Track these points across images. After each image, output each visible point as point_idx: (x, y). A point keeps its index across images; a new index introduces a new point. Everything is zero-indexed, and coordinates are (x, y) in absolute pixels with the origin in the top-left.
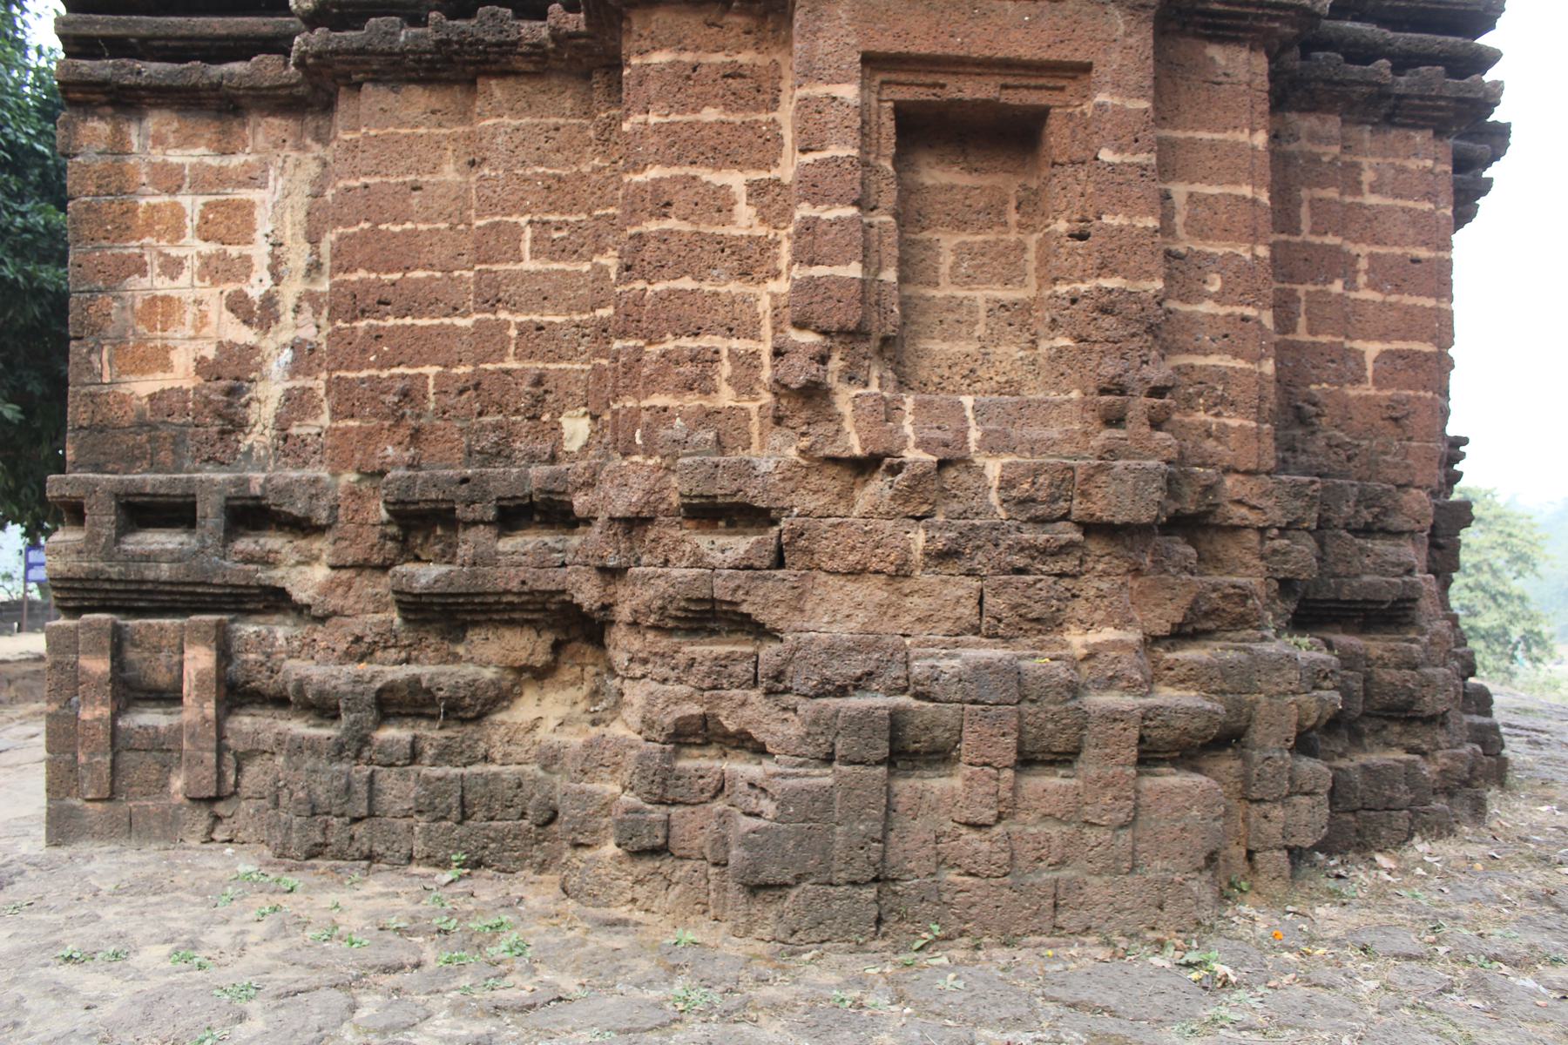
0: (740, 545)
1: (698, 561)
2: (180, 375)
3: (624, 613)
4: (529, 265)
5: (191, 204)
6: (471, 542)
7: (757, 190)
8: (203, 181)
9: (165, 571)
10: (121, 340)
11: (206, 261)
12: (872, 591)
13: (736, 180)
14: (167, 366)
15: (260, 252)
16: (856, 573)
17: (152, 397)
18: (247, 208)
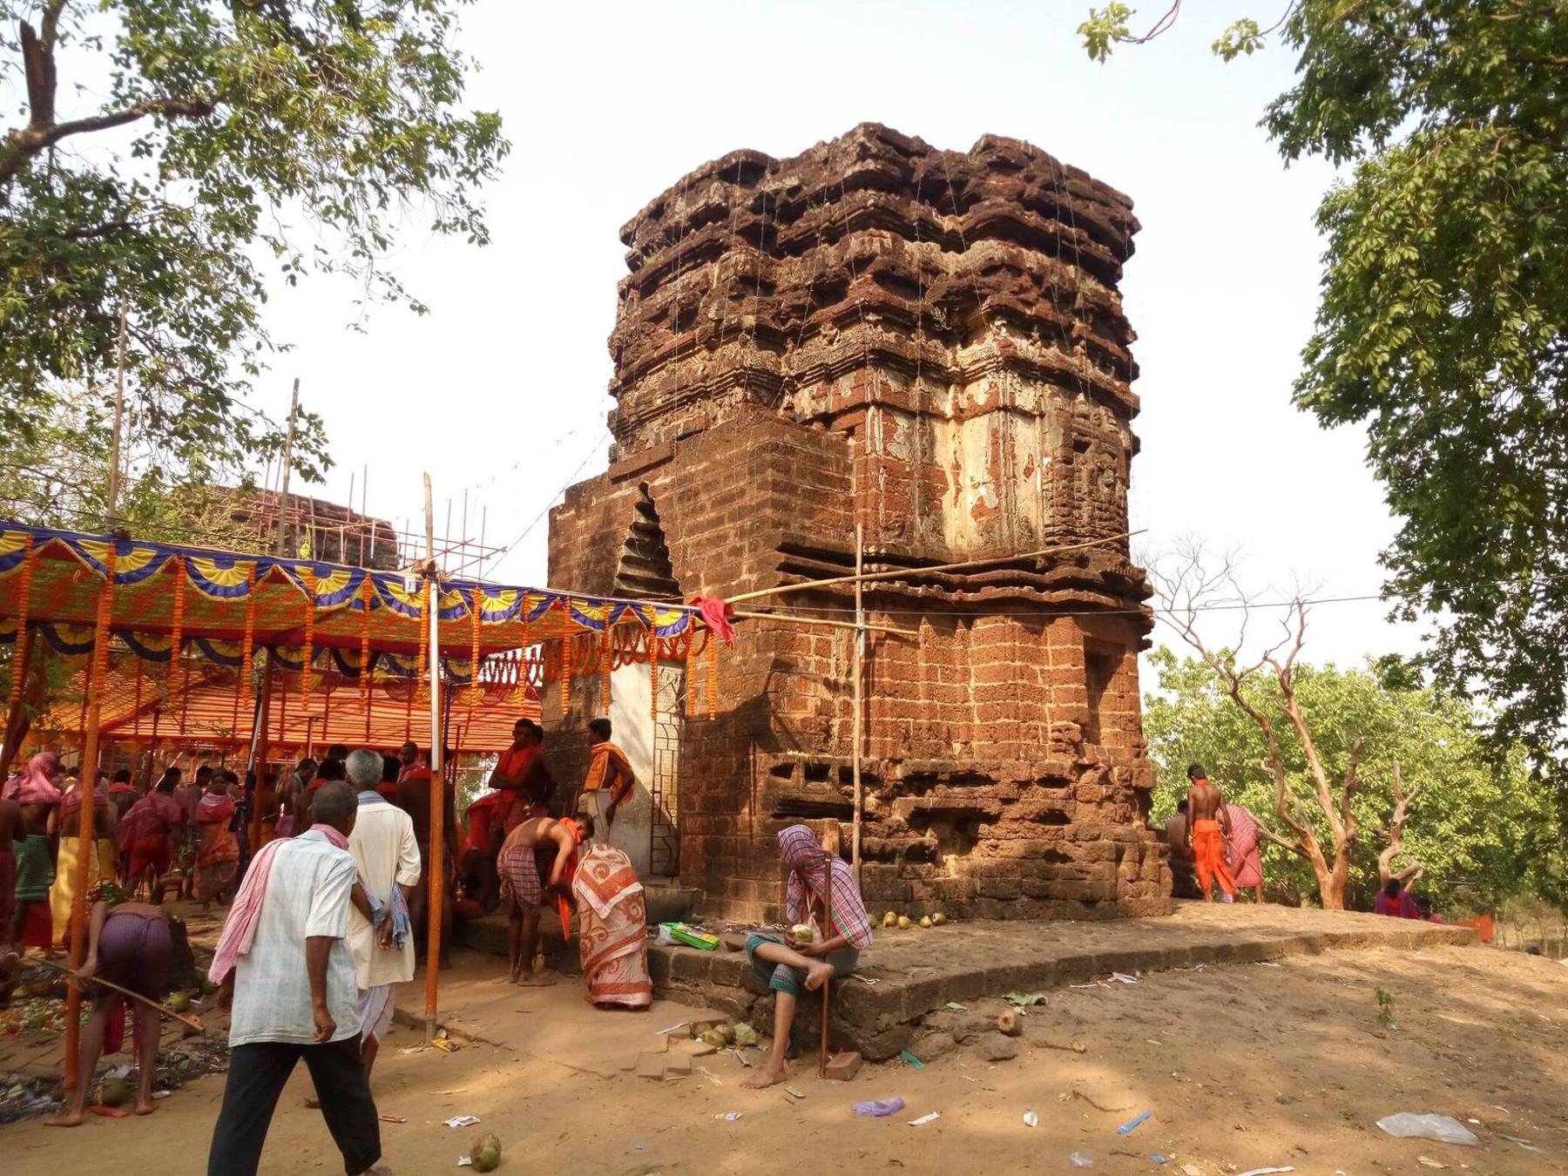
0: (1061, 792)
1: (1046, 796)
2: (809, 712)
3: (1006, 815)
4: (940, 683)
5: (813, 638)
6: (941, 788)
7: (1042, 672)
8: (817, 629)
9: (818, 798)
10: (790, 696)
11: (818, 663)
12: (1092, 807)
13: (1037, 668)
14: (805, 707)
15: (832, 661)
16: (1089, 802)
17: (803, 721)
18: (828, 642)
